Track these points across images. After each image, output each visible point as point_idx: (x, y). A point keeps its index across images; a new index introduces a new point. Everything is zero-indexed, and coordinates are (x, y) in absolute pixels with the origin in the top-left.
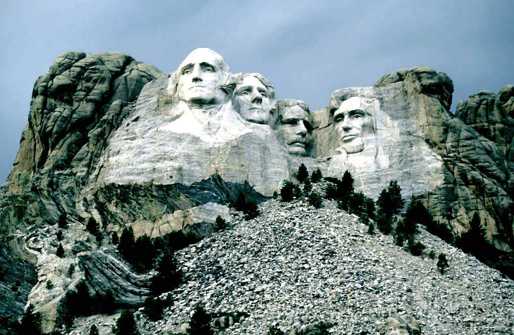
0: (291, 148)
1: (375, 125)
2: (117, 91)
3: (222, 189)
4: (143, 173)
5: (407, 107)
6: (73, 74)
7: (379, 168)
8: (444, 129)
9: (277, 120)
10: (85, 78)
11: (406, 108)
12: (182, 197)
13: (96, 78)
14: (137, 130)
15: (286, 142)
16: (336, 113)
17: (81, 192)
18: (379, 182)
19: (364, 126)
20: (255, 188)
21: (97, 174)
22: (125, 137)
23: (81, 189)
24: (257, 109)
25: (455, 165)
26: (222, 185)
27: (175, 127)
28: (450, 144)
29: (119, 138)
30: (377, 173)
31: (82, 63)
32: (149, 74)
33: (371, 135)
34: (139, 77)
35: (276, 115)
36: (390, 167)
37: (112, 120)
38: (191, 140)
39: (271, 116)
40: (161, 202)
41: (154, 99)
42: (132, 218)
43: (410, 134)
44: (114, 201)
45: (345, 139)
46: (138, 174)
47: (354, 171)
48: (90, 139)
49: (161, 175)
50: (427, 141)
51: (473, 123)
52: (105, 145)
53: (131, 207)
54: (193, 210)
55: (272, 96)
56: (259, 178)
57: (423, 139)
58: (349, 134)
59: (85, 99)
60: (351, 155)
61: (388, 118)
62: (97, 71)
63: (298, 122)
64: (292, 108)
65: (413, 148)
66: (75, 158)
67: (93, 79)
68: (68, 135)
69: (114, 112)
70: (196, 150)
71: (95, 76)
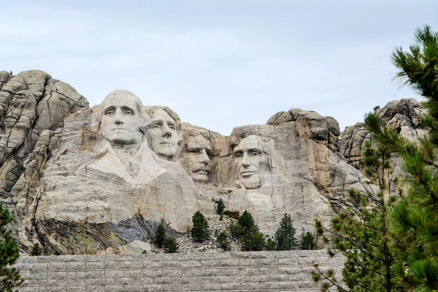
0: (195, 175)
1: (270, 164)
2: (41, 115)
3: (143, 226)
4: (78, 210)
5: (298, 147)
6: (3, 99)
7: (274, 207)
8: (331, 174)
9: (183, 149)
10: (13, 104)
11: (297, 149)
12: (113, 235)
13: (23, 104)
14: (67, 166)
15: (191, 169)
16: (236, 149)
17: (22, 222)
18: (275, 221)
19: (261, 164)
20: (170, 225)
21: (35, 205)
22: (58, 172)
23: (23, 219)
24: (168, 143)
25: (340, 207)
26: (144, 224)
27: (104, 165)
28: (336, 188)
29: (53, 172)
30: (273, 212)
31: (8, 87)
32: (67, 96)
33: (267, 172)
34: (59, 100)
35: (183, 145)
36: (283, 207)
37: (43, 151)
38: (116, 180)
39: (179, 147)
40: (95, 239)
41: (79, 133)
42: (71, 251)
43: (300, 175)
44: (54, 234)
45: (244, 174)
46: (74, 211)
47: (254, 209)
48: (26, 171)
49: (93, 214)
50: (316, 184)
51: (358, 156)
52: (40, 175)
53: (69, 241)
54: (122, 248)
55: (179, 128)
56: (173, 216)
57: (312, 182)
58: (248, 170)
59: (15, 126)
60: (250, 190)
61: (282, 158)
62: (23, 96)
63: (201, 151)
64: (196, 137)
65: (304, 190)
66: (14, 187)
67: (21, 104)
68: (5, 164)
69: (44, 142)
70: (121, 191)
71: (22, 101)
